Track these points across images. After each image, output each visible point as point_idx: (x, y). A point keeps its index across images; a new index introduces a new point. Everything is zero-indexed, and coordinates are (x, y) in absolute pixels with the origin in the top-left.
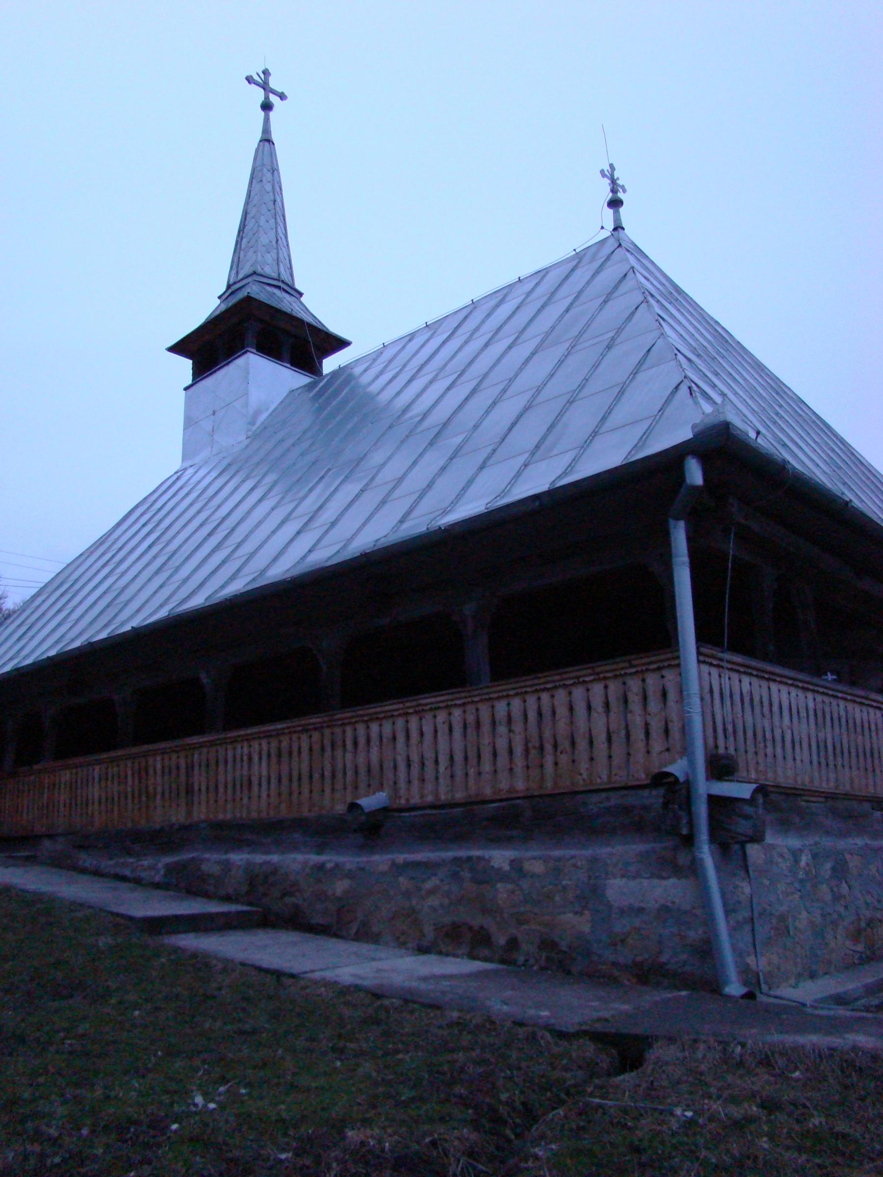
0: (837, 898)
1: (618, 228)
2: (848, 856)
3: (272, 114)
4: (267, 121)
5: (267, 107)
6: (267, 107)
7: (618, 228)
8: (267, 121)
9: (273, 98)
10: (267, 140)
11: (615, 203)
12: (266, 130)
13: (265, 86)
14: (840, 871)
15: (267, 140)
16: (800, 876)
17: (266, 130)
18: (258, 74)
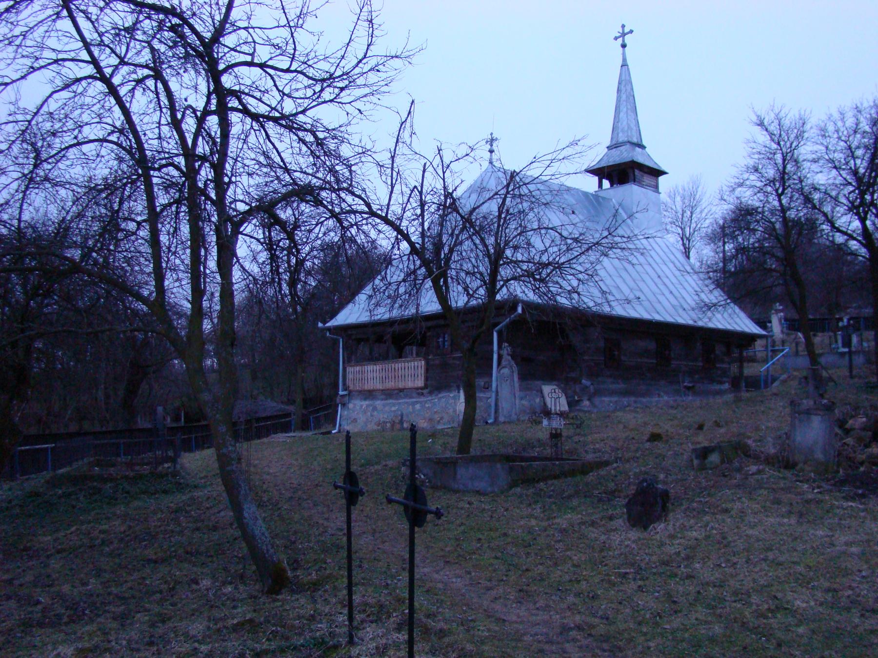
0: (372, 416)
4: (624, 54)
5: (624, 46)
6: (624, 46)
8: (624, 54)
10: (624, 65)
12: (624, 60)
14: (375, 409)
15: (624, 65)
17: (624, 60)
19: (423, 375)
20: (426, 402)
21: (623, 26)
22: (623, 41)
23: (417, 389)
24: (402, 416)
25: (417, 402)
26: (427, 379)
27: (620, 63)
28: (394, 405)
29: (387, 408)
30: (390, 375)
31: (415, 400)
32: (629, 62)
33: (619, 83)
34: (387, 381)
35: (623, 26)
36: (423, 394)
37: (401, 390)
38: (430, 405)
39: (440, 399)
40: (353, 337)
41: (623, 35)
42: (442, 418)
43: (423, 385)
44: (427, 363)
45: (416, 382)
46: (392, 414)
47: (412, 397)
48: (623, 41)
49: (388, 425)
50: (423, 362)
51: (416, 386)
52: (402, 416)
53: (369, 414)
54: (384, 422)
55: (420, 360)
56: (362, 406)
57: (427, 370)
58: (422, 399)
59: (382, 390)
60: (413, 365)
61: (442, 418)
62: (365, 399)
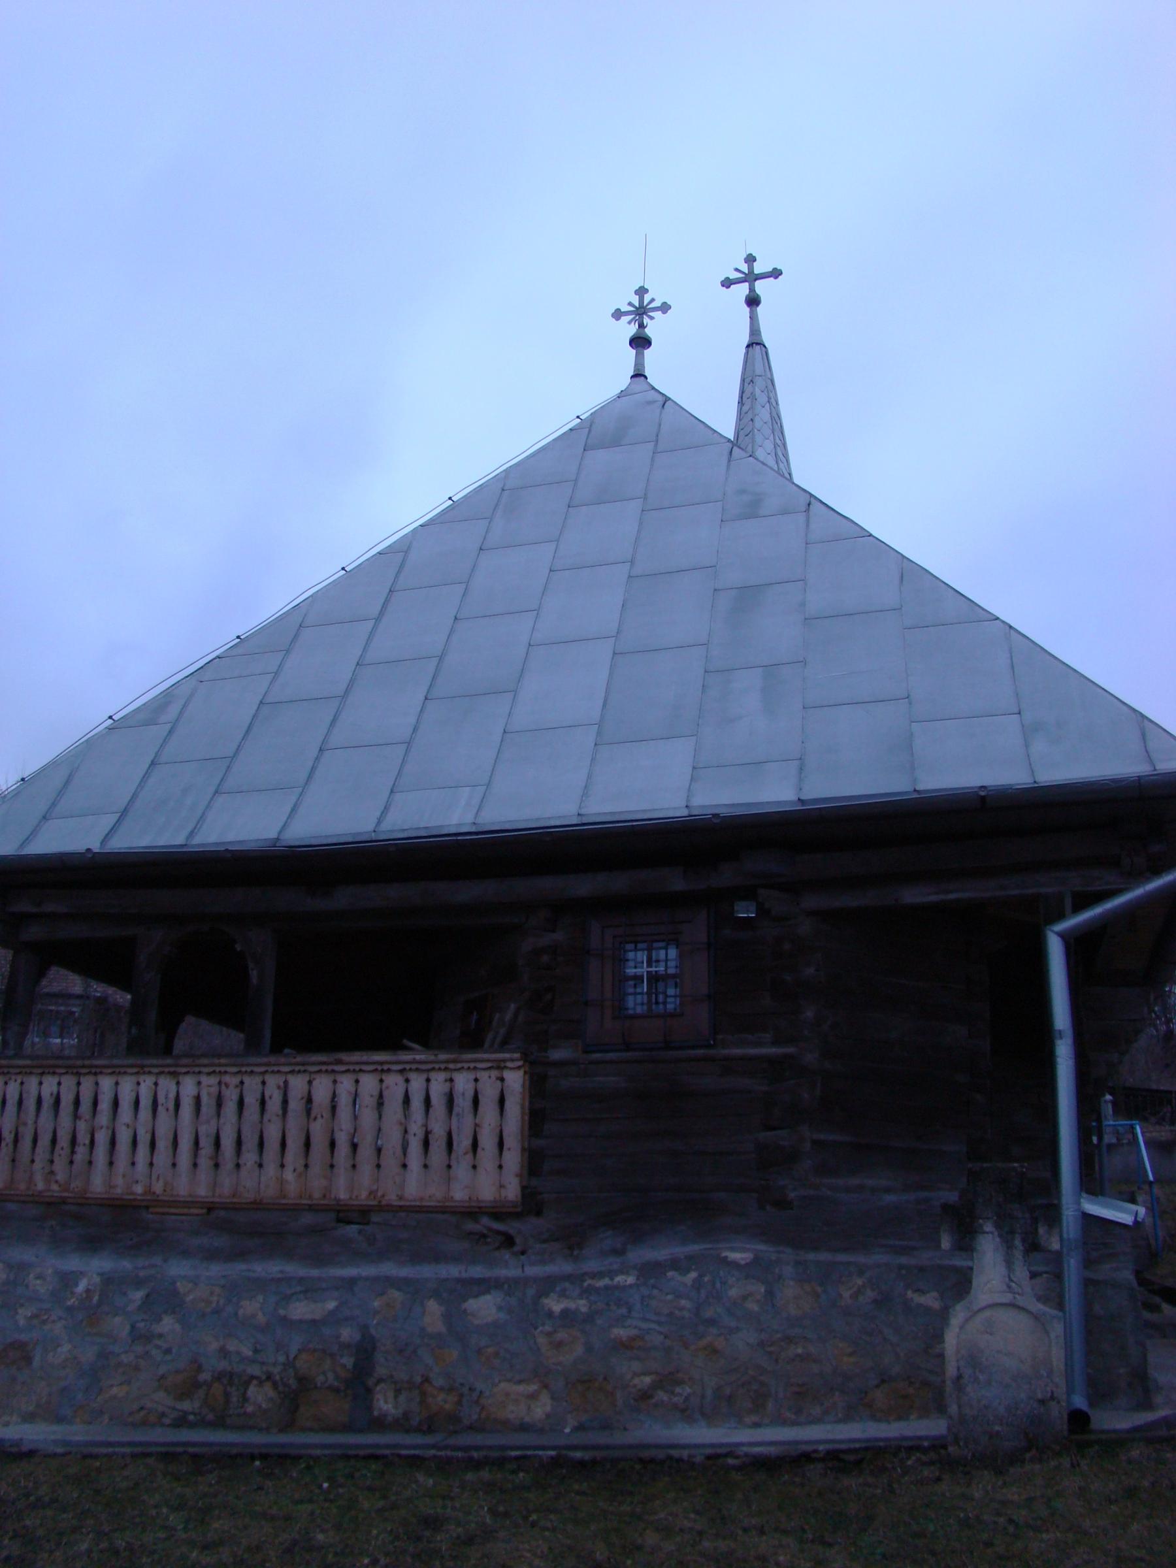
0: (137, 1336)
1: (639, 375)
2: (181, 1287)
3: (760, 309)
4: (753, 318)
5: (753, 301)
6: (753, 301)
7: (639, 375)
8: (753, 318)
9: (761, 287)
10: (755, 343)
11: (640, 342)
12: (755, 330)
13: (751, 278)
15: (755, 343)
16: (69, 1303)
17: (755, 330)
18: (737, 270)
19: (513, 1142)
20: (548, 1285)
21: (750, 259)
22: (752, 289)
23: (472, 1212)
24: (365, 1350)
25: (483, 1286)
26: (534, 1162)
27: (745, 339)
28: (310, 1290)
29: (252, 1307)
30: (273, 1133)
31: (454, 1271)
32: (766, 338)
33: (743, 380)
34: (249, 1157)
35: (750, 259)
36: (508, 1241)
37: (345, 1214)
38: (582, 1305)
39: (651, 1271)
40: (34, 932)
41: (751, 278)
42: (668, 1380)
43: (512, 1191)
44: (537, 1085)
45: (462, 1170)
46: (295, 1343)
47: (438, 1257)
48: (752, 289)
49: (260, 1396)
50: (515, 1080)
51: (459, 1194)
52: (365, 1350)
53: (118, 1325)
54: (226, 1377)
55: (500, 1066)
56: (67, 1280)
57: (535, 1120)
58: (509, 1269)
59: (210, 1208)
60: (438, 1088)
61: (668, 1380)
62: (92, 1244)
